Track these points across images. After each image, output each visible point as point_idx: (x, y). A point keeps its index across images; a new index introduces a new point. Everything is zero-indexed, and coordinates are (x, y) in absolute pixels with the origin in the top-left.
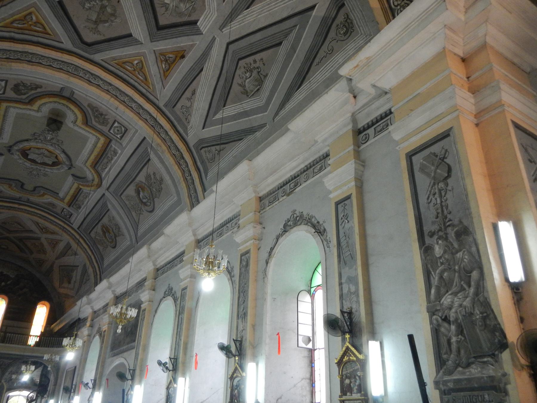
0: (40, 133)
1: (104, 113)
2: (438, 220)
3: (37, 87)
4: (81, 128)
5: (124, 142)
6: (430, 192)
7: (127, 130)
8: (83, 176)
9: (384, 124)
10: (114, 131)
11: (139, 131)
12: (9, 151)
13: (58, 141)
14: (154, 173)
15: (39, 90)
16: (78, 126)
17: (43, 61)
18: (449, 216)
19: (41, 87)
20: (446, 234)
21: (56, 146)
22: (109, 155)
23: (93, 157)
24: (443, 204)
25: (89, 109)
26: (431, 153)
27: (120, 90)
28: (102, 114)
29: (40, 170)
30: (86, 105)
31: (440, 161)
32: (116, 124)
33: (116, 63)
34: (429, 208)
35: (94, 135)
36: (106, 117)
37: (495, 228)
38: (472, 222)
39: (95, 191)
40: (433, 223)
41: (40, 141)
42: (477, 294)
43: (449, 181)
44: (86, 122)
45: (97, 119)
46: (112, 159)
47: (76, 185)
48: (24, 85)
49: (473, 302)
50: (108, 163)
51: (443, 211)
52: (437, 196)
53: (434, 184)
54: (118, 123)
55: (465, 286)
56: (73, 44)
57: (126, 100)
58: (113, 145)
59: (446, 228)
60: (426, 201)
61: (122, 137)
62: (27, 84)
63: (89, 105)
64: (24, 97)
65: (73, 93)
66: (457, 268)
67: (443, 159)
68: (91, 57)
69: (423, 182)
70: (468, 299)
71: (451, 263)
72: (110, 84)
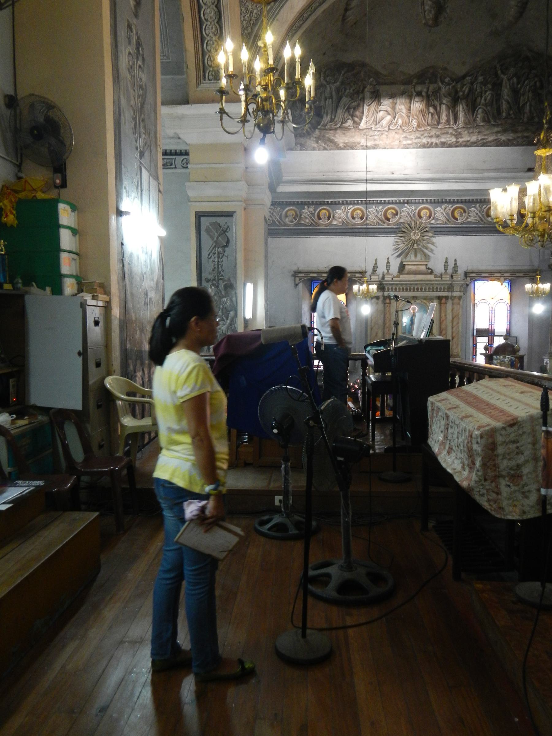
2: (214, 272)
6: (212, 251)
9: (168, 161)
18: (222, 273)
20: (218, 284)
24: (220, 263)
26: (216, 222)
31: (223, 232)
34: (208, 261)
37: (245, 285)
38: (236, 282)
40: (210, 273)
42: (231, 324)
43: (226, 249)
49: (228, 328)
51: (218, 268)
52: (216, 255)
53: (215, 247)
55: (225, 318)
59: (218, 280)
60: (207, 256)
66: (221, 306)
67: (225, 231)
69: (207, 243)
70: (225, 326)
71: (218, 303)
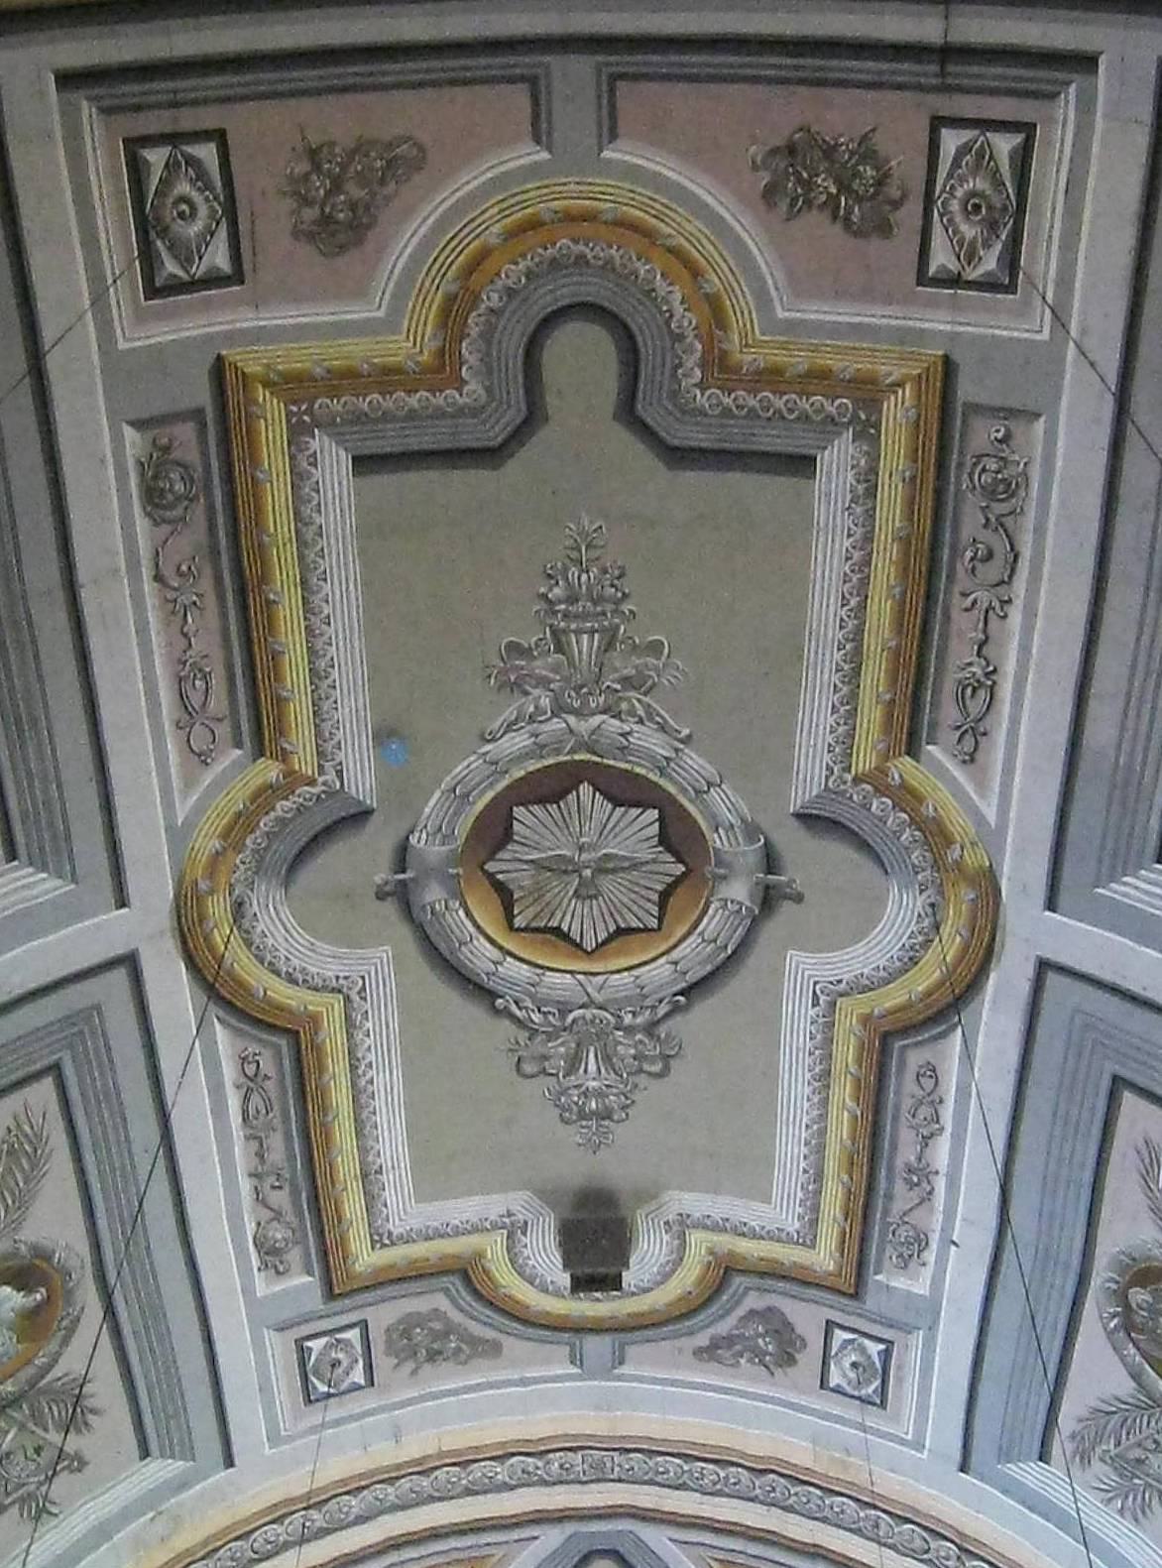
0: (642, 1080)
1: (427, 1367)
3: (709, 1353)
4: (475, 1230)
5: (279, 1349)
7: (309, 1401)
8: (311, 874)
10: (348, 1343)
11: (267, 1451)
12: (771, 861)
13: (544, 1072)
14: (79, 1463)
15: (702, 1339)
16: (495, 1227)
17: (715, 1477)
19: (698, 1352)
21: (536, 1017)
22: (281, 1199)
23: (340, 1098)
25: (490, 1334)
27: (432, 1499)
28: (433, 1356)
29: (559, 710)
30: (507, 1342)
32: (358, 1376)
33: (493, 1555)
35: (406, 1239)
36: (410, 1366)
39: (178, 836)
41: (628, 1019)
44: (467, 1274)
45: (437, 1326)
46: (259, 1198)
47: (304, 761)
48: (758, 1355)
50: (260, 1155)
54: (357, 1388)
56: (639, 1542)
57: (390, 1490)
58: (303, 1282)
61: (302, 1353)
62: (750, 1361)
63: (494, 1349)
64: (753, 1301)
65: (576, 1359)
68: (570, 1528)
72: (469, 1492)
